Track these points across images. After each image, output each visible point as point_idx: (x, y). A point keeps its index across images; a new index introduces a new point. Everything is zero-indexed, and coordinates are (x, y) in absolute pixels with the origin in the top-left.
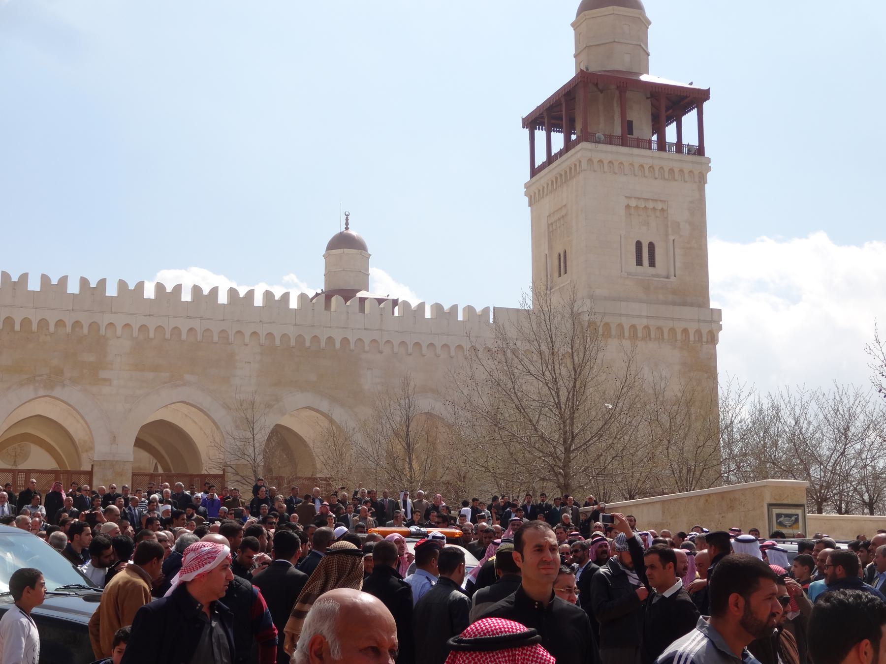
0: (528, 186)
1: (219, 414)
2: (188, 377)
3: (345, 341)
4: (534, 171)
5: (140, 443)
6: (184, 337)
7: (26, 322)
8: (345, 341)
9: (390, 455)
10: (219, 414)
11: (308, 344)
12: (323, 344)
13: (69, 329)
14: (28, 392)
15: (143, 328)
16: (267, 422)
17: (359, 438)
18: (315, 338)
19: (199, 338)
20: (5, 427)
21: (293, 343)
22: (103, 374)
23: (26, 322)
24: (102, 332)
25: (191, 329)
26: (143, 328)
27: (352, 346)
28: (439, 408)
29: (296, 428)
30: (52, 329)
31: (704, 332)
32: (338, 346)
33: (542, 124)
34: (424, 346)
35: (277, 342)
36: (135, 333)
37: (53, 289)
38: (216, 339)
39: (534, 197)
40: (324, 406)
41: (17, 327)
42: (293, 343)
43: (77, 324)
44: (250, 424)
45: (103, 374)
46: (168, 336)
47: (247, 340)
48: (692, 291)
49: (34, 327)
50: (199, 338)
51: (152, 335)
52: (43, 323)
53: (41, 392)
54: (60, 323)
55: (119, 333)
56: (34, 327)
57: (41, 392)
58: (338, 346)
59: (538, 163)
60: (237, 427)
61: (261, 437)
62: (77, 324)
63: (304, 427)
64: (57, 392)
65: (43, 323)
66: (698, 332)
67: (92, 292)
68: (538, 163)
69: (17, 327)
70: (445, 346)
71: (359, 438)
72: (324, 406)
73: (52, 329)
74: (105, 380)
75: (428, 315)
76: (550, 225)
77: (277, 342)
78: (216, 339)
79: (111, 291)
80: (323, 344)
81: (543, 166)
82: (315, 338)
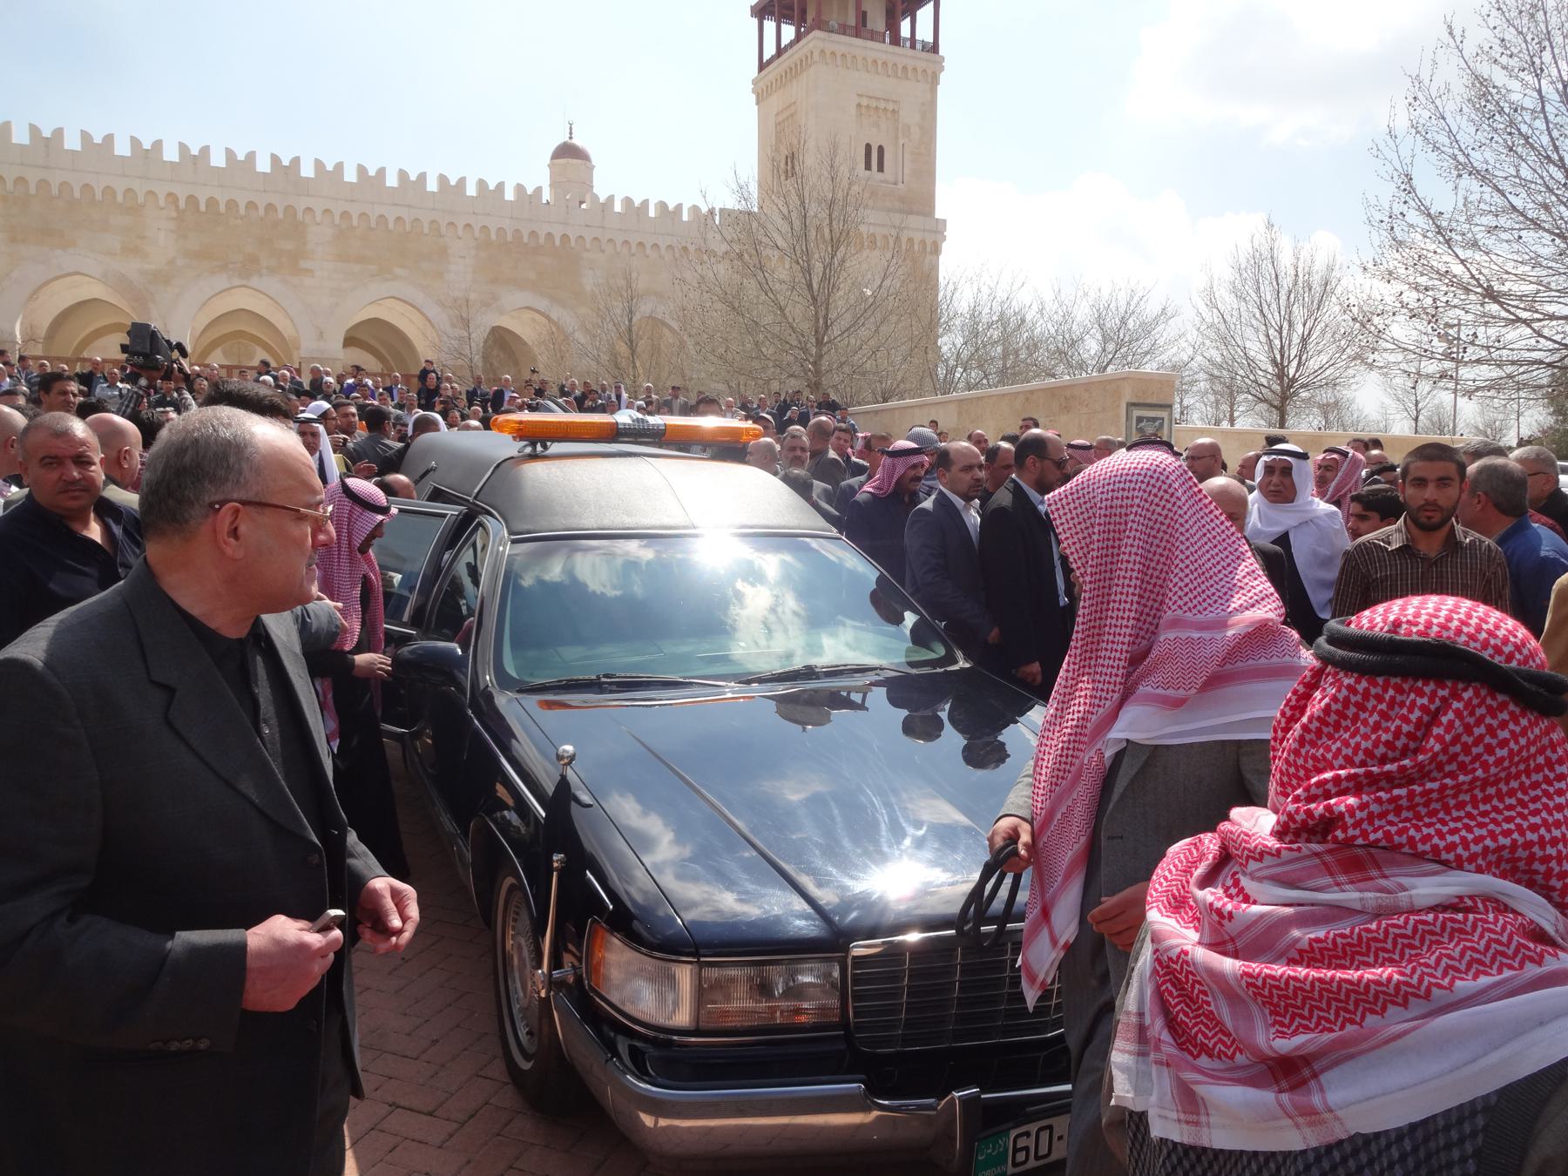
0: (755, 82)
1: (434, 312)
2: (399, 271)
3: (565, 237)
4: (762, 66)
5: (350, 341)
6: (391, 226)
7: (212, 202)
8: (565, 237)
9: (614, 355)
10: (434, 312)
11: (525, 240)
12: (542, 241)
13: (261, 212)
14: (221, 282)
15: (345, 215)
16: (486, 321)
17: (580, 337)
18: (533, 233)
19: (408, 228)
20: (204, 320)
21: (509, 238)
22: (304, 264)
23: (212, 202)
24: (300, 216)
25: (399, 218)
26: (345, 215)
27: (573, 243)
28: (661, 311)
29: (518, 331)
30: (242, 211)
31: (929, 242)
32: (557, 242)
33: (772, 14)
34: (648, 247)
35: (493, 237)
36: (337, 220)
37: (240, 167)
38: (426, 231)
39: (762, 94)
40: (542, 304)
41: (203, 208)
42: (509, 238)
43: (270, 207)
44: (466, 323)
45: (304, 264)
46: (373, 225)
47: (460, 232)
48: (919, 201)
49: (222, 208)
50: (408, 228)
51: (355, 223)
52: (232, 204)
53: (237, 282)
54: (251, 205)
55: (318, 219)
56: (222, 208)
57: (237, 282)
58: (557, 242)
59: (766, 57)
60: (453, 326)
61: (479, 335)
62: (270, 207)
63: (524, 328)
64: (255, 281)
65: (232, 204)
66: (923, 242)
67: (286, 172)
68: (766, 57)
69: (203, 208)
70: (670, 247)
71: (580, 337)
72: (542, 304)
73: (242, 211)
74: (307, 270)
75: (652, 213)
76: (778, 124)
77: (493, 237)
78: (426, 231)
79: (307, 171)
80: (542, 241)
81: (770, 61)
82: (533, 233)
